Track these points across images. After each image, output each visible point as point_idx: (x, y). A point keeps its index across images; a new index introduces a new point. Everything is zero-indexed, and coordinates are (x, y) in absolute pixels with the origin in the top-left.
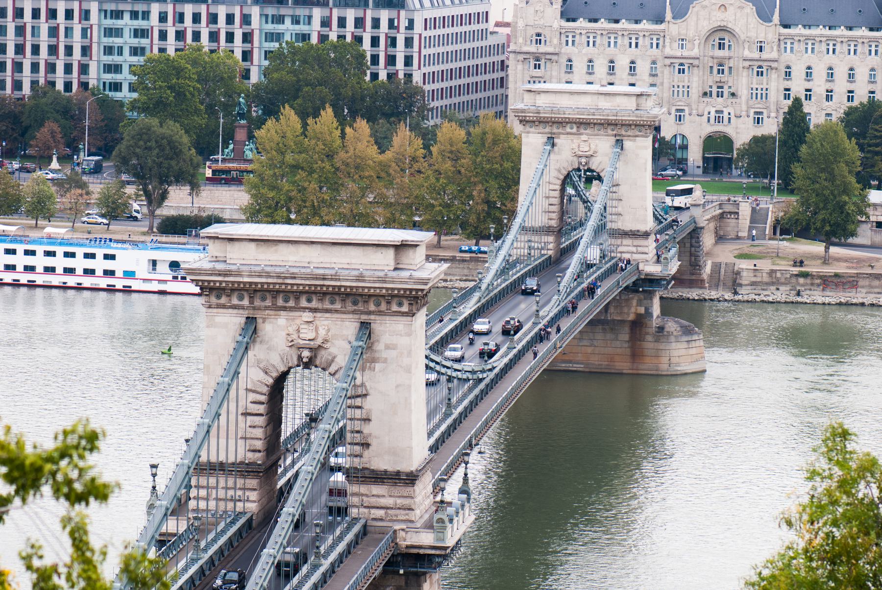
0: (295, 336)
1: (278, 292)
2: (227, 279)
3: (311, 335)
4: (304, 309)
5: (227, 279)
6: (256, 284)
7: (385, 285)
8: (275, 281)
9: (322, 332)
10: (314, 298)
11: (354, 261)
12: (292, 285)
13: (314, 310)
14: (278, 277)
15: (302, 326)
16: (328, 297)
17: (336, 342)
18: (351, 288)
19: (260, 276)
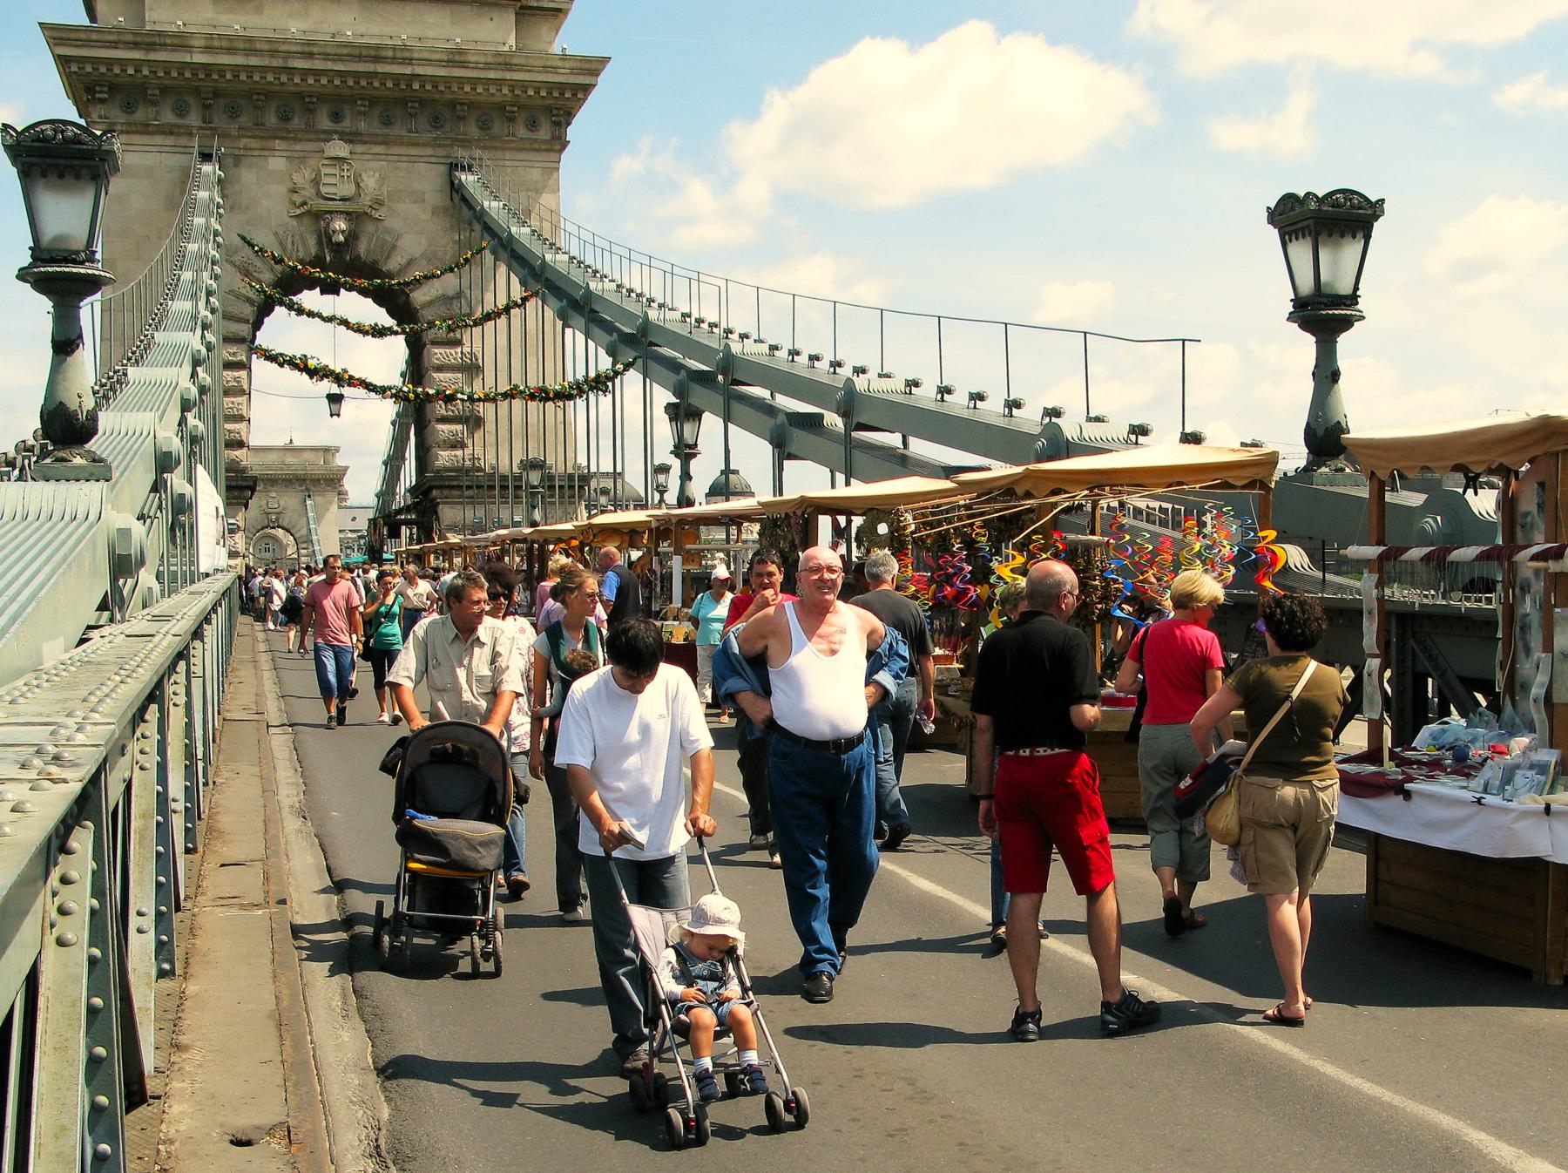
0: (309, 192)
1: (269, 95)
2: (152, 56)
3: (348, 189)
4: (327, 136)
5: (152, 56)
6: (221, 70)
7: (508, 75)
8: (266, 62)
9: (370, 182)
10: (347, 109)
11: (431, 34)
12: (306, 72)
13: (350, 138)
14: (273, 53)
15: (324, 171)
16: (377, 111)
17: (400, 207)
18: (435, 80)
19: (231, 51)
